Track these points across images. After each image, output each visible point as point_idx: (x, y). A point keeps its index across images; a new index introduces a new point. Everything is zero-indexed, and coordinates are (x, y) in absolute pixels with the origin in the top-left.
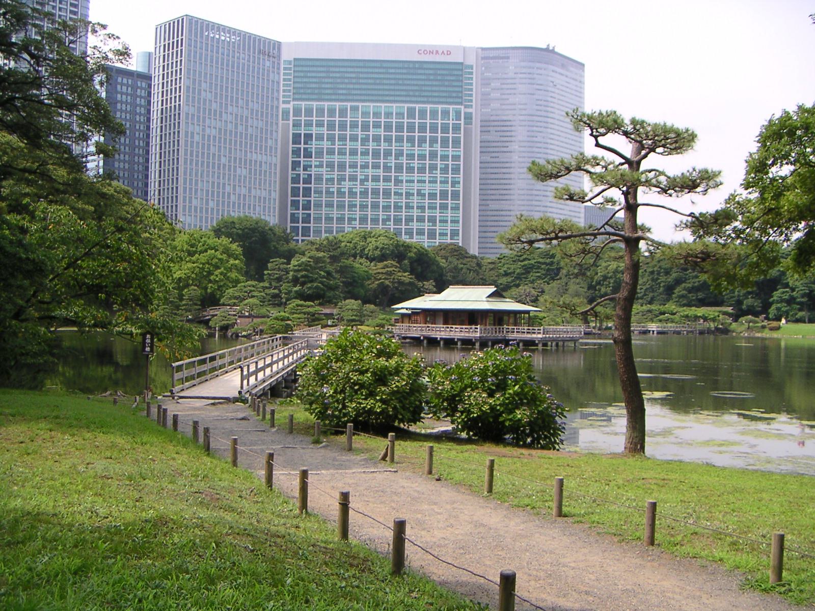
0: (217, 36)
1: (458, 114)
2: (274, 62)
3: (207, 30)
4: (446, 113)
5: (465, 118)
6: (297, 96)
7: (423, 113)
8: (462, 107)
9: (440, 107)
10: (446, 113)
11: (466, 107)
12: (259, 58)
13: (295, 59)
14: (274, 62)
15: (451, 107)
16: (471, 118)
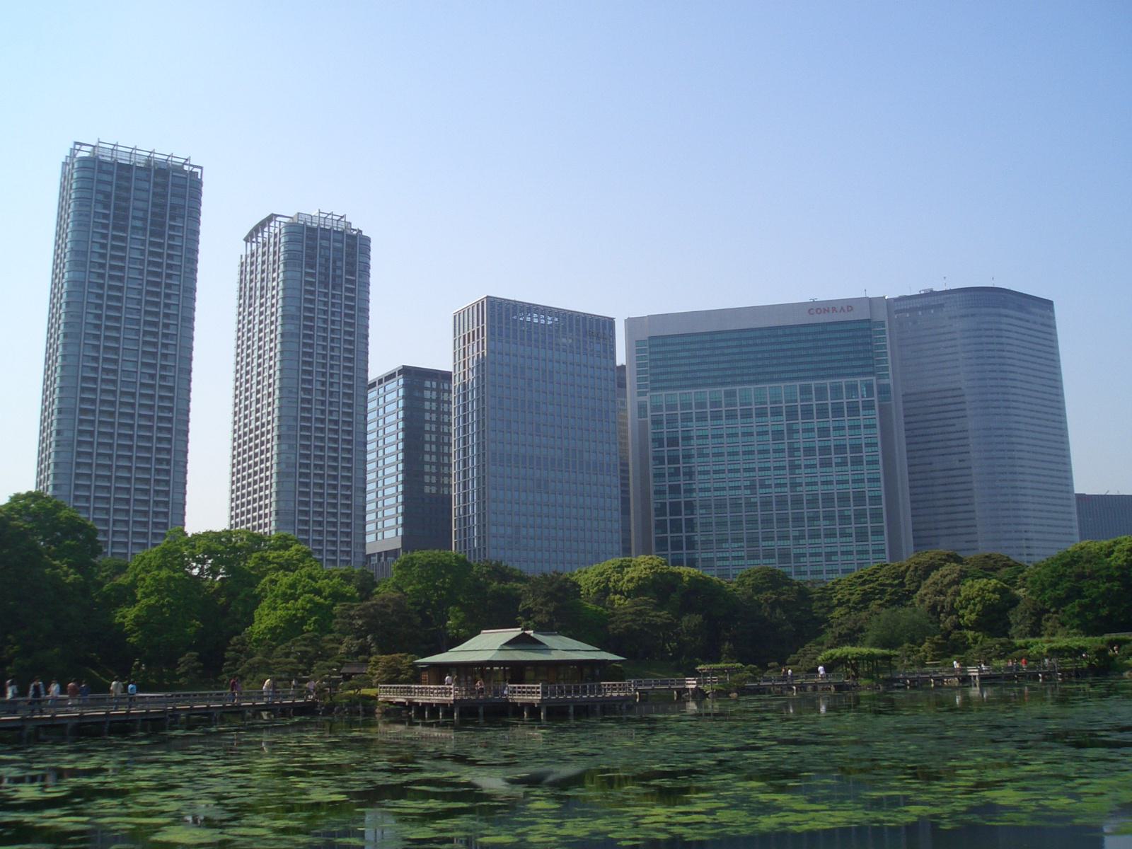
0: (528, 319)
1: (869, 387)
2: (605, 345)
3: (515, 314)
4: (852, 388)
5: (879, 393)
6: (657, 385)
7: (821, 391)
8: (874, 378)
9: (843, 381)
10: (852, 388)
11: (880, 377)
12: (585, 342)
13: (650, 338)
14: (605, 345)
15: (859, 380)
16: (889, 392)
